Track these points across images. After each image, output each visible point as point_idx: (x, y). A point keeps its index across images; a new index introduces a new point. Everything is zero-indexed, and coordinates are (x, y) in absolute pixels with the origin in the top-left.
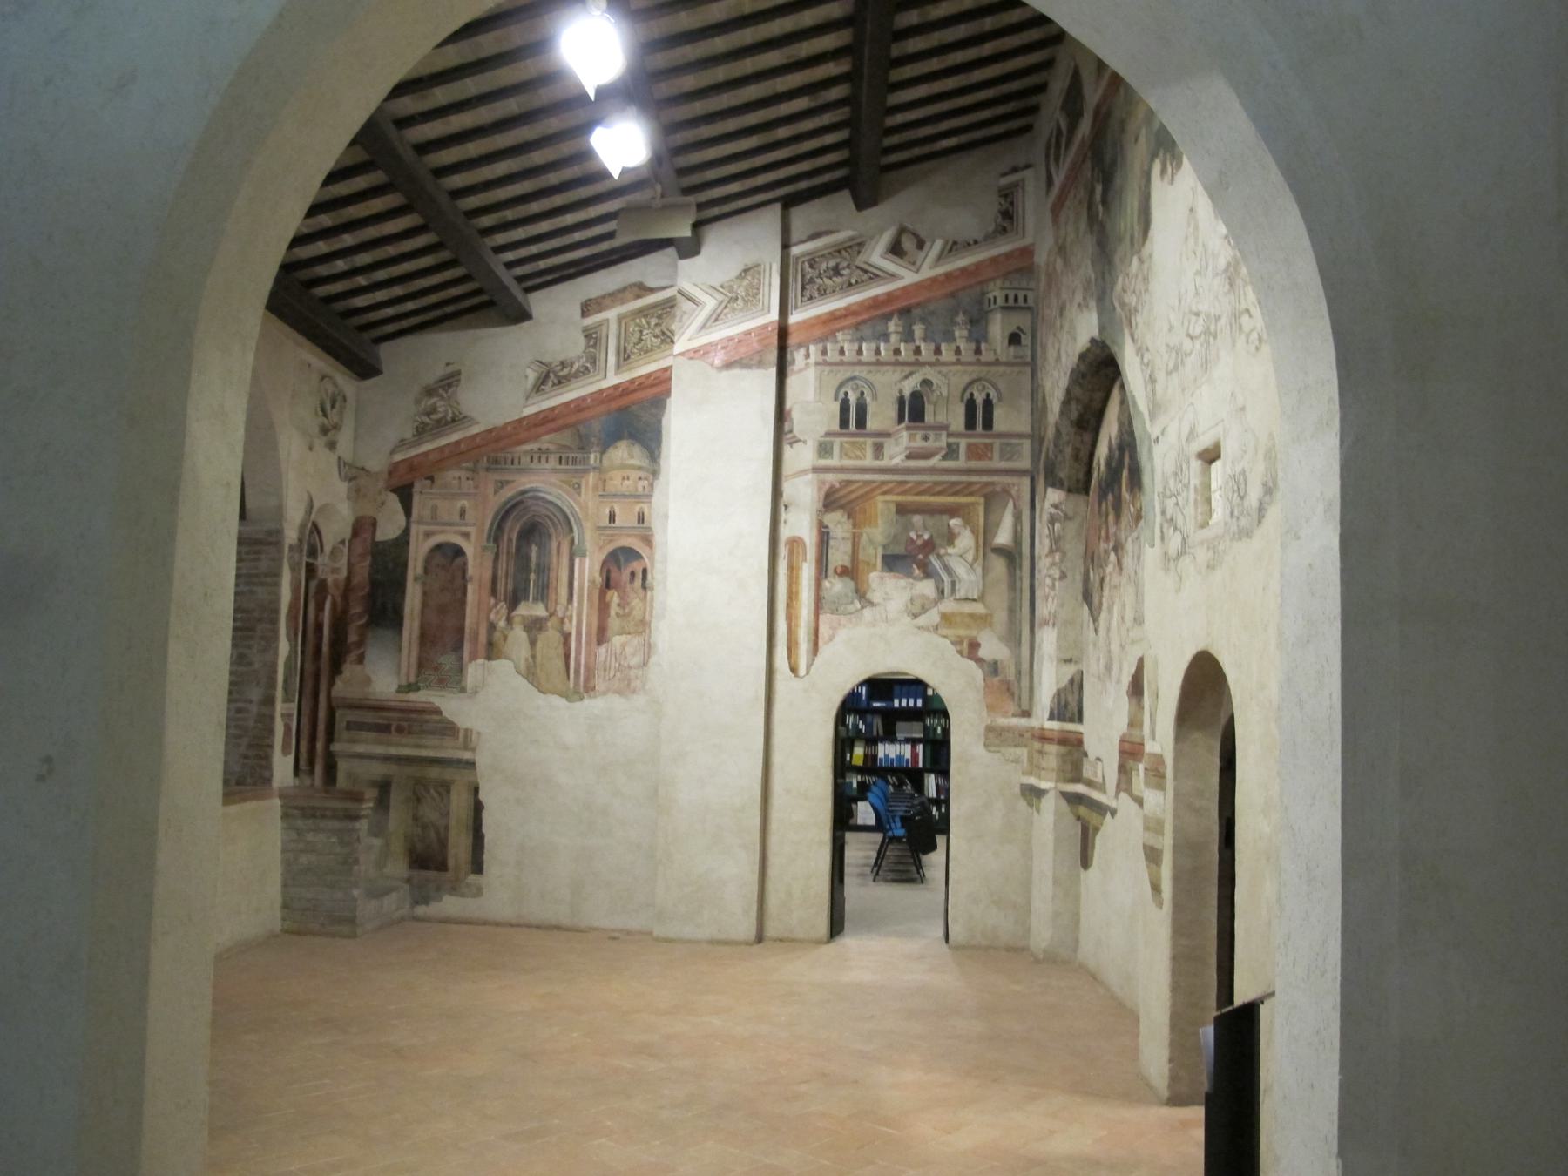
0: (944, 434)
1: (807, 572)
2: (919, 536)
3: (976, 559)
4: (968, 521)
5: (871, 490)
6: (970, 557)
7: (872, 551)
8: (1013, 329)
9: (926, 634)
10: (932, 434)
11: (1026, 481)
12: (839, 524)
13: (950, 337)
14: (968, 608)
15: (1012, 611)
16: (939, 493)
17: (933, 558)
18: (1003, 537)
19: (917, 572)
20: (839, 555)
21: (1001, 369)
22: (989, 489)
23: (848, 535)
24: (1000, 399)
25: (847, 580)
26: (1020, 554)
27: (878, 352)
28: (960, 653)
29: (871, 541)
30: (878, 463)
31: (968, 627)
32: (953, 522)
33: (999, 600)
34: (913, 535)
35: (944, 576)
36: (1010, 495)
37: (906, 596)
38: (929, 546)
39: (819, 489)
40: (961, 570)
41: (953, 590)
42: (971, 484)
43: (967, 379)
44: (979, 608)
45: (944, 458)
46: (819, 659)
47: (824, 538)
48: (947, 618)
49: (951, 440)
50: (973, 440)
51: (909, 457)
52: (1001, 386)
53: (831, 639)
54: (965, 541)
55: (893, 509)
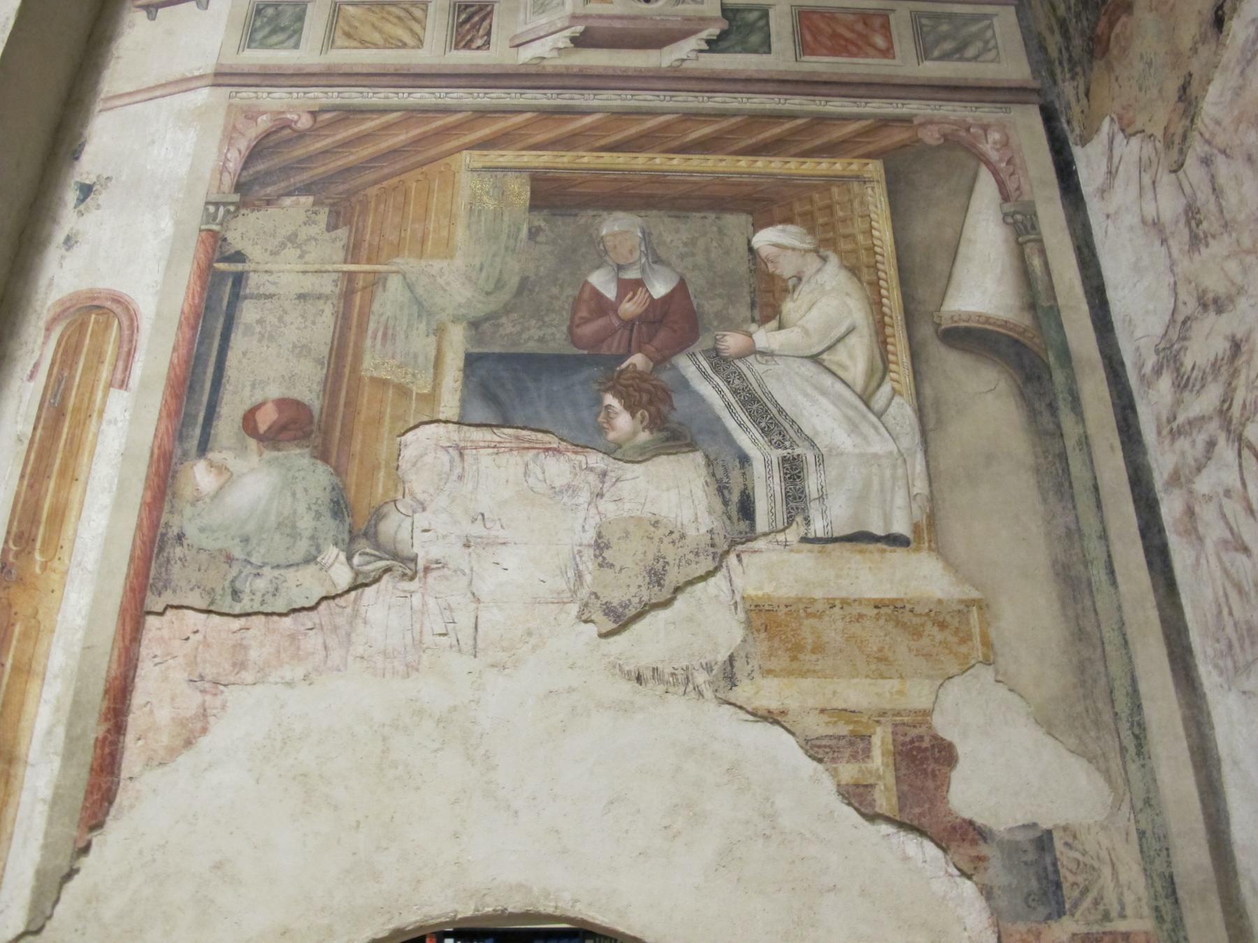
1: (123, 426)
2: (629, 287)
3: (881, 367)
4: (828, 234)
5: (434, 137)
6: (855, 359)
7: (423, 344)
9: (678, 706)
12: (292, 254)
14: (871, 578)
15: (1075, 582)
16: (704, 146)
17: (689, 367)
18: (981, 288)
19: (623, 422)
20: (271, 362)
22: (898, 136)
23: (327, 285)
25: (298, 457)
26: (1065, 356)
28: (856, 796)
29: (422, 308)
31: (882, 664)
33: (1006, 533)
34: (603, 282)
35: (748, 440)
36: (982, 158)
37: (576, 529)
38: (675, 323)
39: (230, 136)
40: (821, 415)
41: (795, 500)
42: (821, 120)
44: (922, 578)
45: (713, 45)
46: (111, 844)
47: (220, 290)
48: (763, 618)
53: (190, 734)
54: (827, 303)
55: (520, 190)
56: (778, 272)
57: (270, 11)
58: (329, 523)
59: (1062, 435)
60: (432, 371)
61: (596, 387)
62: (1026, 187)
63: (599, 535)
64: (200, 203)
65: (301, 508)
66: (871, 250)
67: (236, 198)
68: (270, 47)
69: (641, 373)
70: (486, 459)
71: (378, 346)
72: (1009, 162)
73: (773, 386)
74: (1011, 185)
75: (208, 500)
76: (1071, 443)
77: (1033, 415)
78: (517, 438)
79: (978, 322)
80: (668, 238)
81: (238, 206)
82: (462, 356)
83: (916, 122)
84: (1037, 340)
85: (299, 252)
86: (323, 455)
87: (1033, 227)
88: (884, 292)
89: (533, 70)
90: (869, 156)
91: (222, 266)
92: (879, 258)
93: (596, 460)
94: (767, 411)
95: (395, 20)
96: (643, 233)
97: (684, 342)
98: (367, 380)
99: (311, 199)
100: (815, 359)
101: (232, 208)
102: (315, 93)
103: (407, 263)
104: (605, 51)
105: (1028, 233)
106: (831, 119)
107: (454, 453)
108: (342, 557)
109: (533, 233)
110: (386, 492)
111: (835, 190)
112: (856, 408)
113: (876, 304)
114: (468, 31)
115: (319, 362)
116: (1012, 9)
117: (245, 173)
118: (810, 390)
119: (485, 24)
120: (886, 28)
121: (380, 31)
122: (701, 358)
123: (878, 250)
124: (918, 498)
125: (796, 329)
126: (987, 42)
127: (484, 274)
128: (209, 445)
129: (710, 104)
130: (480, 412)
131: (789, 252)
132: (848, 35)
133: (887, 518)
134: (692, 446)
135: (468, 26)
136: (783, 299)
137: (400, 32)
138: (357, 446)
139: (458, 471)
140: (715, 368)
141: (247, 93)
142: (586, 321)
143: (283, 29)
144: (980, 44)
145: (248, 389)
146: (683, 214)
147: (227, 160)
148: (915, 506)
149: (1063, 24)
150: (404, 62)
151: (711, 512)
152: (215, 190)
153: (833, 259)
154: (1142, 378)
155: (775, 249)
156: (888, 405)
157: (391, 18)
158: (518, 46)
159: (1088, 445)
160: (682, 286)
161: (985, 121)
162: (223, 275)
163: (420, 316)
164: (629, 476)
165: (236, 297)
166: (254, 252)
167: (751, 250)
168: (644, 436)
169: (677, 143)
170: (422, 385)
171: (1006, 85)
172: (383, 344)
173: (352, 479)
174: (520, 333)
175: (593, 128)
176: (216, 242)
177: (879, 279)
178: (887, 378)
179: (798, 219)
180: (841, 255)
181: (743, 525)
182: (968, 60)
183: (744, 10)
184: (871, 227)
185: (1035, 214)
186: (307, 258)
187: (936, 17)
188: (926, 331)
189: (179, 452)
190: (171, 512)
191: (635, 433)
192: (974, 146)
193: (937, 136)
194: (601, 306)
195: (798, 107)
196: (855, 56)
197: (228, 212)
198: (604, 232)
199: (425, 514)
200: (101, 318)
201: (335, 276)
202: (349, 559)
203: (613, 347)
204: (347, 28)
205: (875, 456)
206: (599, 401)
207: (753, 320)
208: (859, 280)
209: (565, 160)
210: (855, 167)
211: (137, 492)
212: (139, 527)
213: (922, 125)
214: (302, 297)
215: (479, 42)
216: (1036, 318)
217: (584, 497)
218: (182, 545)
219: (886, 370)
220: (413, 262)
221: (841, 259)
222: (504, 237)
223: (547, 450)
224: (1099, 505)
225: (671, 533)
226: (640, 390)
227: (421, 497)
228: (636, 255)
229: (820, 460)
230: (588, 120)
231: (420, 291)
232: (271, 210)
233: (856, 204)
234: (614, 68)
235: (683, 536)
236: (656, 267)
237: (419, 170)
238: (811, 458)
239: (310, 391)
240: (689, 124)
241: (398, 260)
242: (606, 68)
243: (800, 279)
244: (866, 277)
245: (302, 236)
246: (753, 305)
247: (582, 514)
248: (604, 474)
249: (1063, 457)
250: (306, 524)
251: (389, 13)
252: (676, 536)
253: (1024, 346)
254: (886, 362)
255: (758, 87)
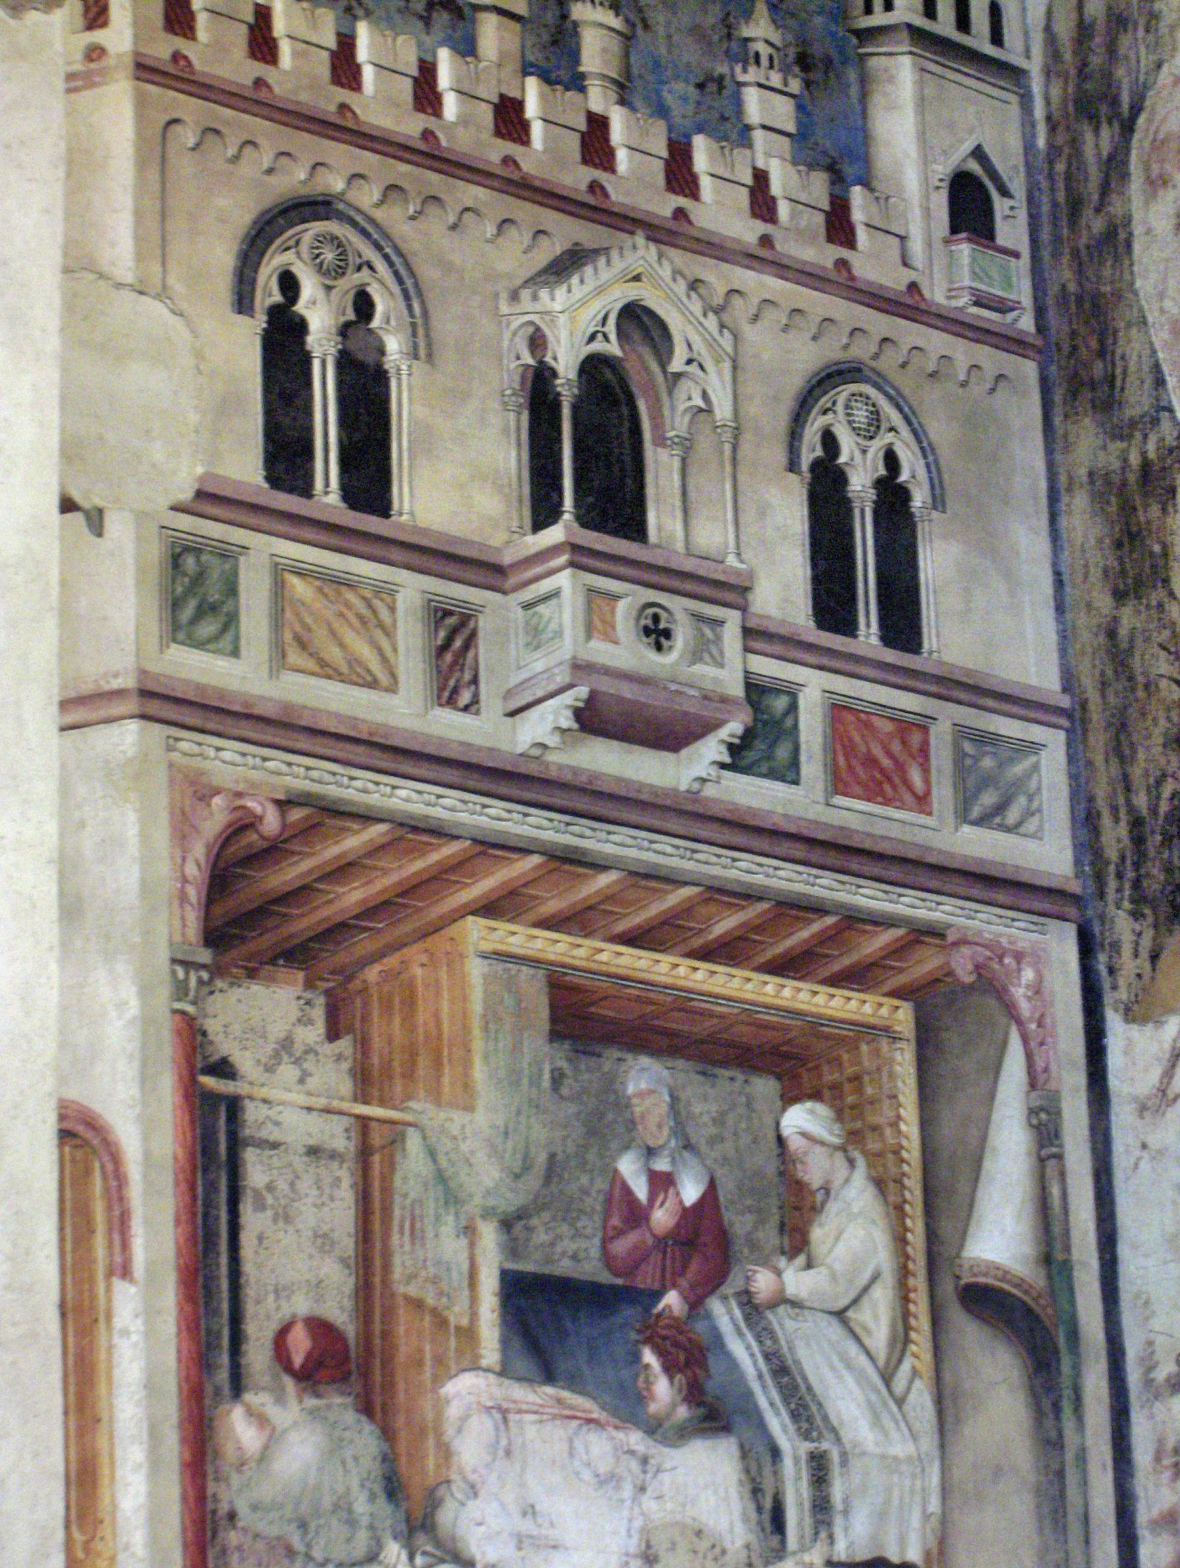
0: (733, 619)
2: (662, 1183)
3: (901, 1339)
6: (877, 1317)
7: (450, 1247)
8: (957, 156)
10: (679, 609)
11: (1060, 947)
13: (734, 131)
17: (723, 1314)
19: (663, 1390)
21: (937, 342)
23: (336, 1135)
24: (938, 501)
25: (339, 1405)
26: (1074, 1335)
27: (426, 94)
30: (449, 727)
32: (800, 1119)
35: (778, 1424)
36: (1010, 1009)
38: (704, 1248)
42: (854, 921)
43: (806, 357)
45: (739, 757)
49: (766, 667)
50: (843, 685)
51: (592, 720)
52: (939, 430)
54: (855, 1232)
56: (806, 1178)
57: (190, 562)
58: (383, 1507)
59: (1062, 1447)
60: (466, 1293)
61: (633, 1336)
62: (1053, 1067)
63: (648, 1546)
64: (163, 956)
65: (355, 1483)
66: (897, 1151)
67: (205, 956)
68: (200, 645)
69: (675, 1319)
70: (530, 1431)
71: (407, 1247)
72: (1040, 1025)
73: (802, 1353)
74: (1040, 1064)
75: (253, 1464)
76: (1069, 1455)
77: (1039, 1415)
78: (559, 1401)
79: (995, 1277)
80: (697, 1109)
81: (217, 970)
82: (497, 1273)
83: (950, 939)
84: (1050, 1311)
85: (298, 1073)
86: (366, 1409)
87: (1057, 1135)
88: (909, 1222)
89: (532, 769)
90: (895, 994)
91: (209, 1081)
92: (906, 1168)
93: (635, 1439)
94: (796, 1387)
95: (356, 622)
96: (671, 1096)
97: (713, 1280)
98: (400, 1301)
99: (301, 975)
100: (840, 1315)
101: (205, 975)
102: (277, 761)
103: (420, 1108)
104: (615, 743)
105: (1052, 1145)
106: (863, 921)
107: (498, 1416)
108: (404, 1556)
109: (557, 1079)
110: (438, 1467)
111: (864, 1048)
112: (878, 1392)
113: (900, 1240)
114: (451, 667)
115: (343, 1261)
116: (1061, 736)
117: (218, 910)
118: (835, 1360)
119: (471, 654)
120: (924, 751)
121: (342, 646)
122: (733, 1303)
123: (904, 1154)
124: (933, 1519)
125: (823, 1270)
126: (1030, 799)
127: (510, 1145)
128: (244, 1382)
129: (733, 874)
130: (523, 1364)
131: (818, 1149)
132: (886, 762)
133: (903, 1551)
134: (726, 1429)
135: (448, 657)
136: (809, 1223)
137: (365, 651)
138: (401, 1397)
139: (504, 1442)
140: (747, 1318)
141: (188, 742)
142: (620, 1233)
143: (214, 608)
144: (1023, 800)
145: (271, 1298)
146: (709, 1068)
147: (185, 880)
148: (928, 1530)
149: (1137, 823)
150: (379, 718)
151: (745, 1519)
152: (178, 938)
153: (861, 1162)
154: (1148, 1382)
155: (804, 1141)
156: (909, 1389)
157: (350, 615)
158: (512, 714)
159: (1084, 1461)
160: (712, 1186)
161: (1021, 945)
162: (210, 1099)
163: (446, 1203)
164: (668, 1466)
165: (236, 1143)
166: (244, 1062)
167: (781, 1141)
168: (683, 1412)
169: (697, 942)
170: (457, 1315)
171: (1044, 883)
172: (413, 1244)
173: (402, 1447)
174: (553, 1244)
175: (610, 897)
176: (194, 1038)
177: (905, 1201)
178: (908, 1354)
179: (827, 1093)
180: (874, 1158)
181: (775, 1541)
182: (1008, 830)
183: (771, 690)
184: (899, 1117)
185: (1059, 1113)
186: (313, 1083)
187: (985, 739)
188: (948, 1288)
189: (209, 1389)
190: (217, 1479)
191: (674, 1406)
192: (1005, 989)
193: (970, 967)
194: (636, 1215)
195: (826, 894)
196: (887, 802)
197: (201, 982)
198: (631, 1089)
199: (478, 1502)
200: (79, 1154)
201: (346, 1121)
202: (411, 1558)
203: (646, 1279)
204: (298, 628)
205: (895, 1458)
206: (636, 1357)
207: (783, 1253)
208: (885, 1200)
209: (581, 952)
210: (884, 1011)
211: (172, 1447)
212: (184, 1498)
213: (956, 944)
214: (313, 1151)
215: (465, 697)
216: (1050, 1277)
217: (627, 1491)
218: (234, 1527)
219: (907, 1340)
220: (430, 1108)
221: (870, 1166)
222: (525, 1081)
223: (589, 1421)
224: (1087, 1542)
225: (713, 1546)
226: (676, 1344)
227: (472, 1477)
228: (666, 1131)
229: (844, 1463)
230: (604, 880)
231: (443, 1162)
232: (255, 988)
233: (885, 1074)
234: (628, 782)
235: (724, 1552)
236: (686, 1154)
237: (421, 945)
238: (835, 1456)
239: (342, 1309)
240: (712, 908)
241: (412, 1104)
242: (619, 780)
243: (828, 1192)
244: (892, 1199)
245: (298, 1049)
246: (782, 1227)
247: (626, 1513)
248: (645, 1461)
249: (1061, 1474)
250: (361, 1506)
251: (349, 606)
252: (717, 1550)
253: (1037, 1318)
254: (907, 1328)
255: (785, 847)
